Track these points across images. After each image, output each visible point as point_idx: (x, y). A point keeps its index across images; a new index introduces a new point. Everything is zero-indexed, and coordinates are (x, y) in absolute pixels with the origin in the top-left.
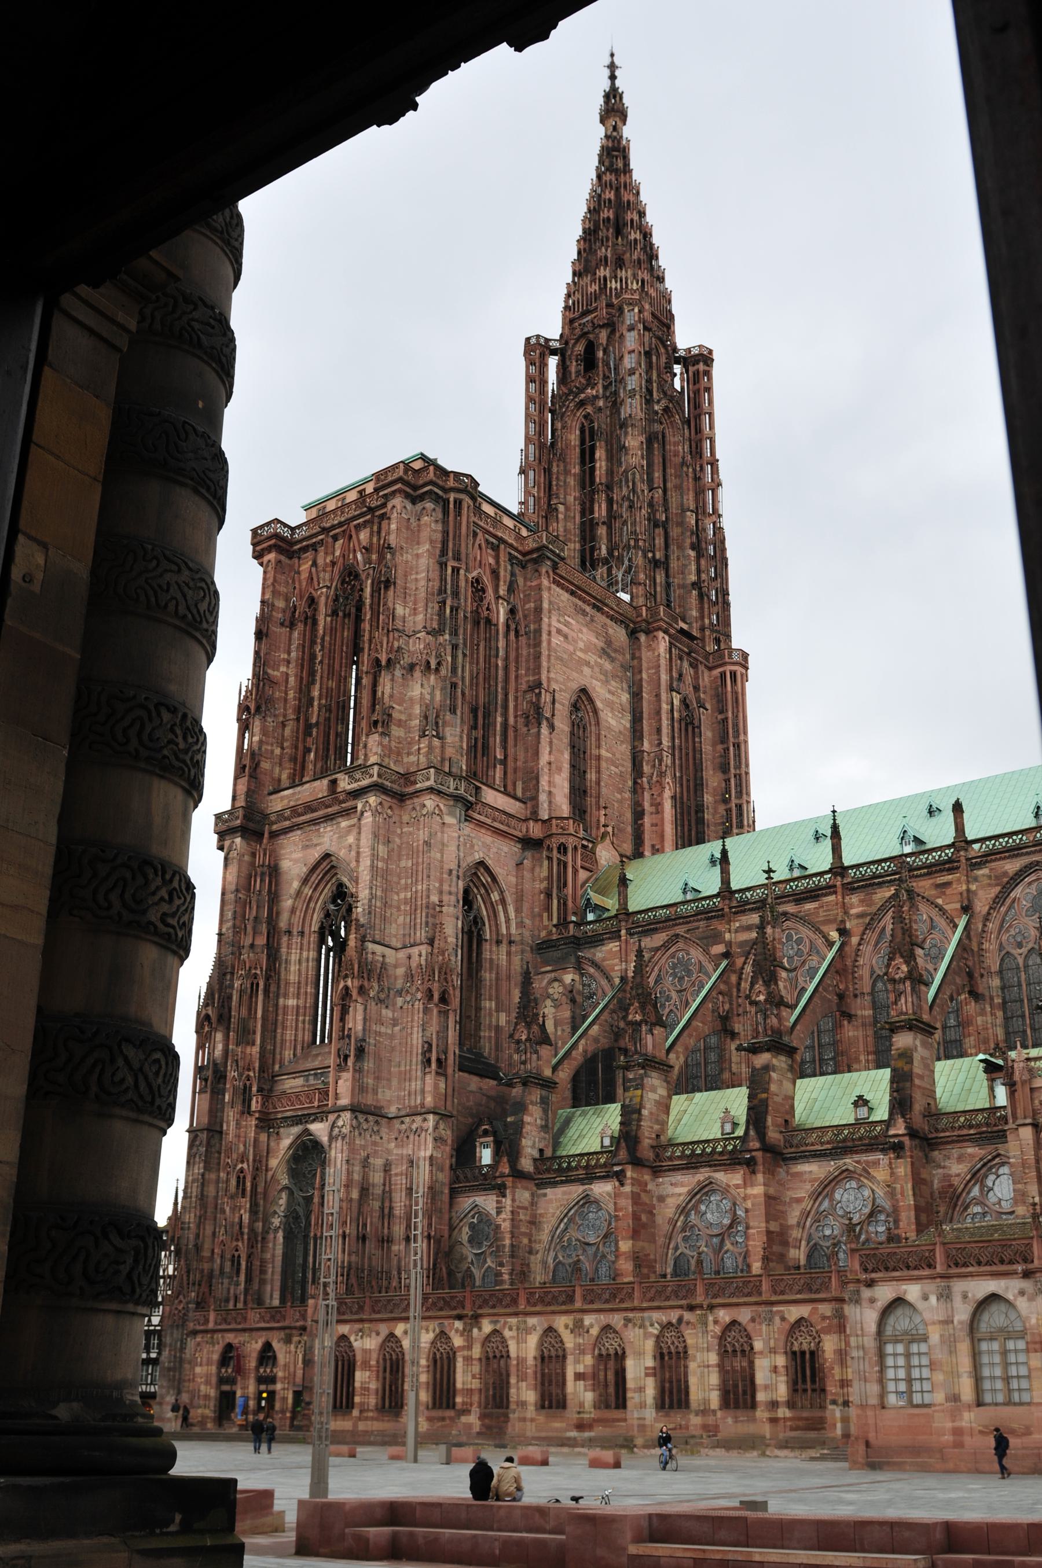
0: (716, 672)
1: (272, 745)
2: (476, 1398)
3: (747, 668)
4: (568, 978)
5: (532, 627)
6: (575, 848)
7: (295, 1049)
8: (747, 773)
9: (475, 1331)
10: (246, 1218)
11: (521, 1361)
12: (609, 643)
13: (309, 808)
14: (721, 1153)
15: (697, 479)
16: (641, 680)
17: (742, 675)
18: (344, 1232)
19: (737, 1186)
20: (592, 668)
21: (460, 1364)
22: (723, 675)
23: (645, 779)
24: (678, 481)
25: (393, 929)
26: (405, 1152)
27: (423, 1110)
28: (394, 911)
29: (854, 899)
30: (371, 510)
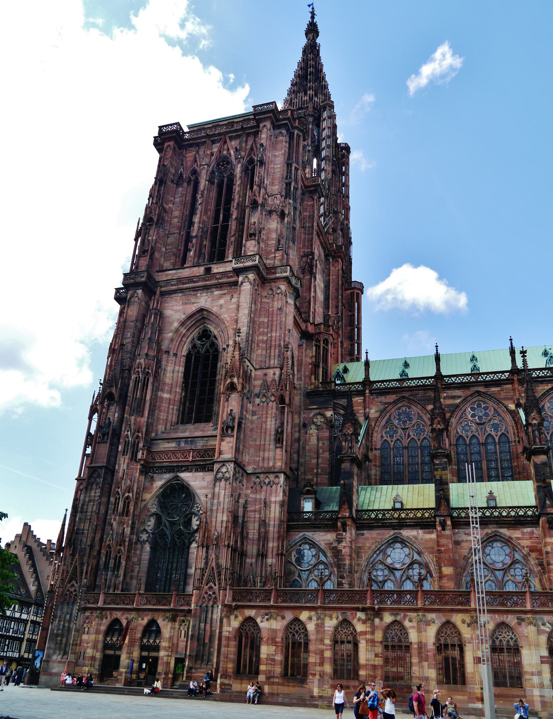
0: (348, 292)
1: (161, 245)
2: (379, 672)
4: (329, 414)
5: (307, 224)
6: (331, 343)
9: (377, 621)
10: (128, 531)
11: (421, 646)
13: (190, 279)
14: (506, 516)
16: (329, 279)
18: (229, 544)
19: (518, 539)
21: (362, 645)
22: (352, 294)
25: (254, 356)
26: (258, 496)
27: (276, 470)
28: (256, 345)
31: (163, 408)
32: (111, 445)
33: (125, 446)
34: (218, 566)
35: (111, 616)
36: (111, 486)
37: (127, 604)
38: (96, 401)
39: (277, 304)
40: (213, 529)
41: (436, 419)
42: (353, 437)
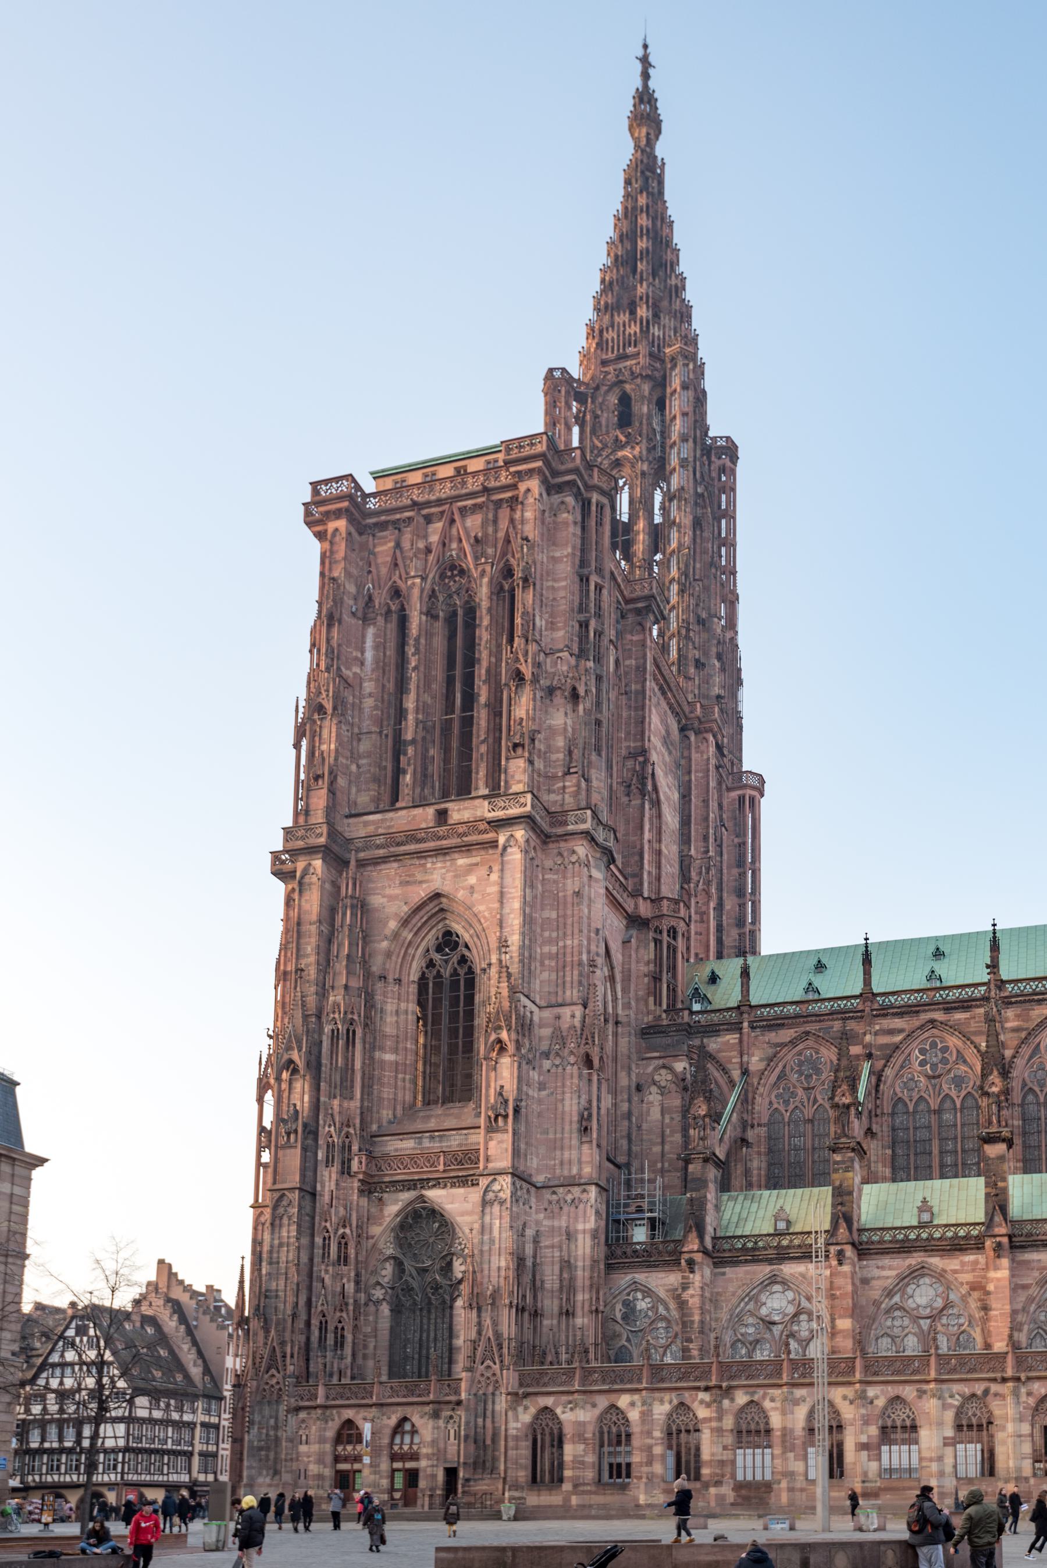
4: (680, 1066)
7: (395, 1109)
10: (350, 1287)
25: (536, 985)
26: (556, 1223)
27: (583, 1181)
28: (538, 964)
31: (386, 1080)
32: (304, 1149)
33: (328, 1152)
34: (498, 1335)
35: (339, 1417)
36: (313, 1218)
37: (363, 1398)
38: (266, 1069)
39: (571, 885)
40: (486, 1280)
41: (840, 1087)
42: (707, 1120)
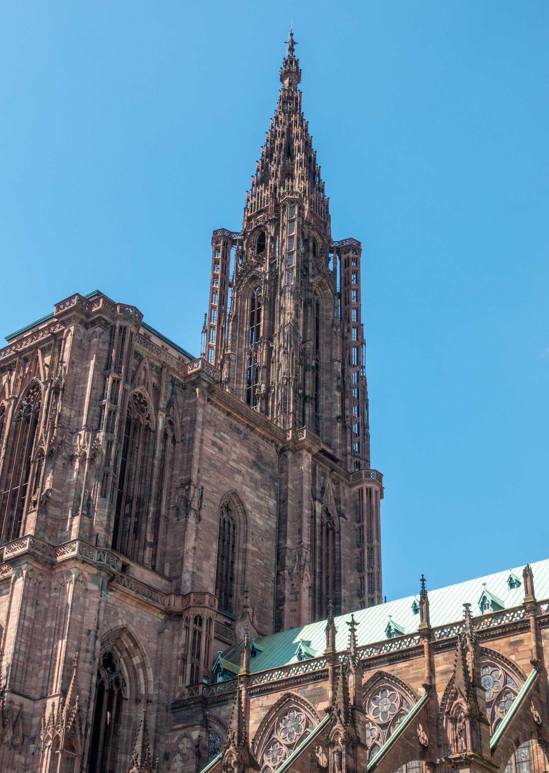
0: (355, 489)
3: (382, 489)
4: (195, 734)
5: (187, 436)
8: (379, 573)
12: (260, 457)
15: (344, 338)
16: (287, 489)
17: (376, 492)
20: (243, 476)
22: (361, 491)
23: (286, 571)
24: (328, 339)
25: (32, 682)
28: (36, 666)
29: (439, 658)
30: (54, 335)
